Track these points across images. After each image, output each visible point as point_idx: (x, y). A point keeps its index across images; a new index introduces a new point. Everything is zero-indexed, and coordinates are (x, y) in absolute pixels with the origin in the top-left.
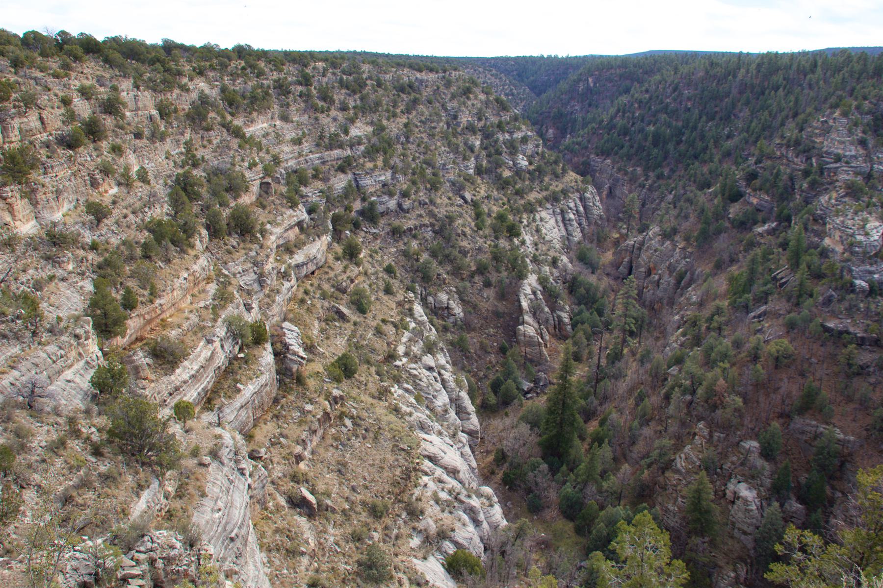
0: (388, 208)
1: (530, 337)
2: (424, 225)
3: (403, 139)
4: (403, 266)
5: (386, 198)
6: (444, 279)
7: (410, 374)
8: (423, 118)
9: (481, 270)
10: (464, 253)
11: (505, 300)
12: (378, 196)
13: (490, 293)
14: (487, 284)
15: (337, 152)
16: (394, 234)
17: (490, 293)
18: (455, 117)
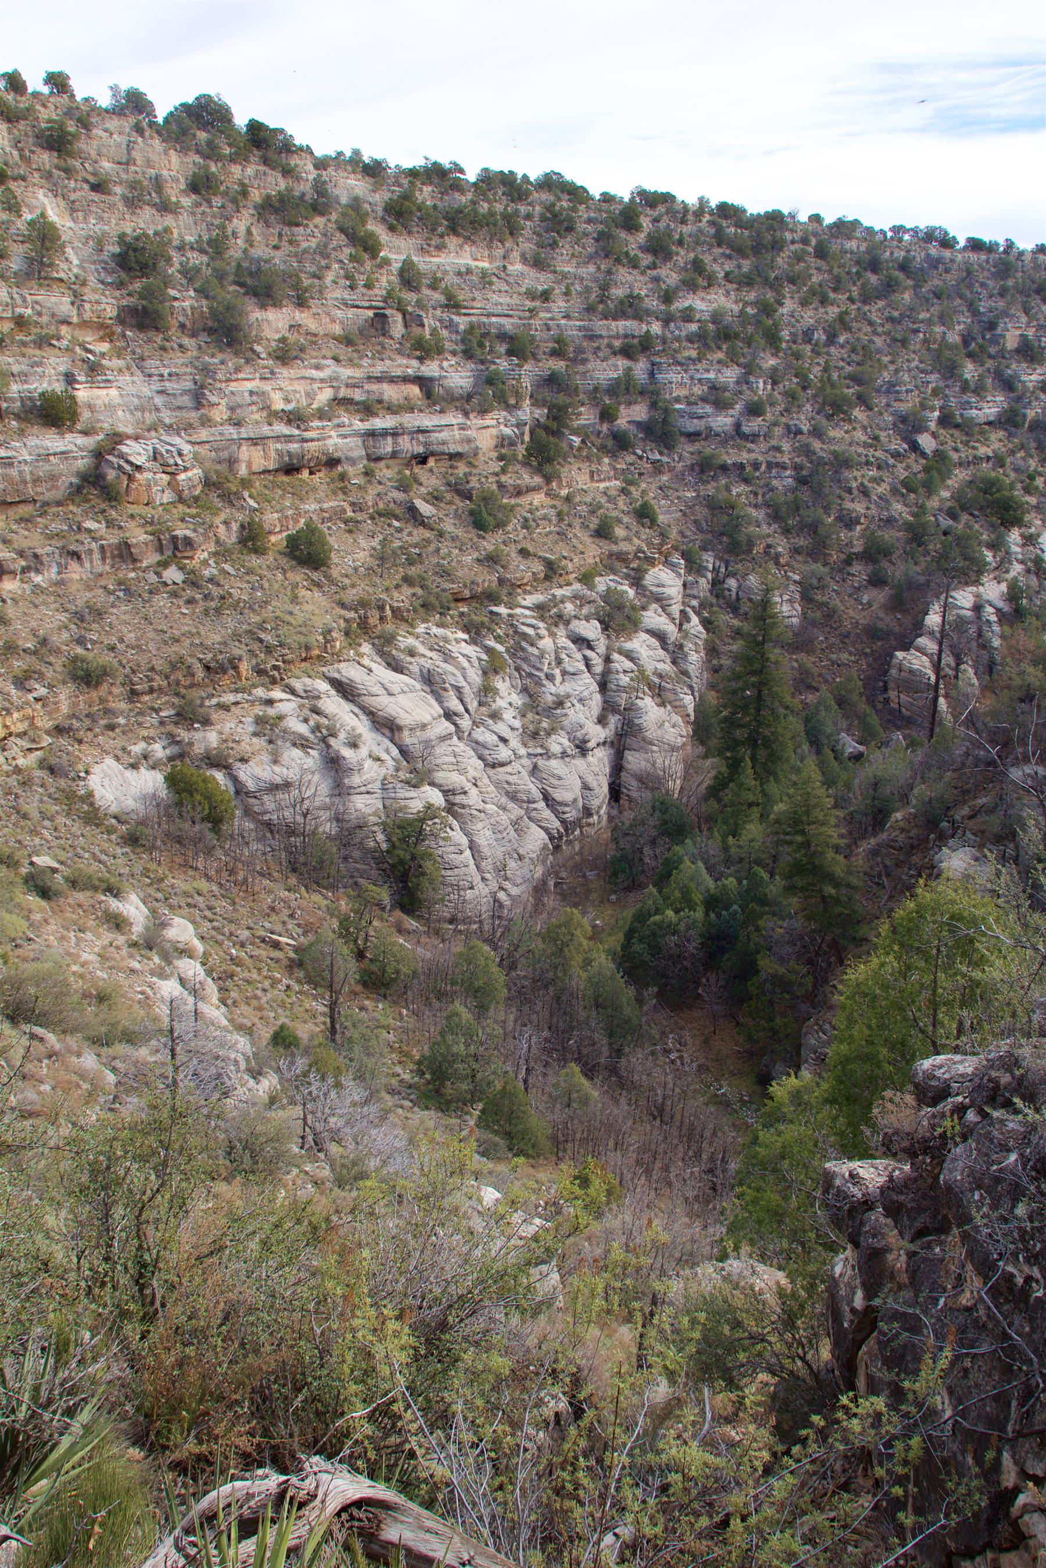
0: (710, 429)
1: (911, 671)
2: (777, 465)
3: (820, 336)
4: (695, 522)
5: (709, 409)
6: (778, 556)
7: (516, 632)
8: (896, 314)
9: (874, 553)
10: (848, 522)
11: (904, 611)
12: (689, 404)
13: (878, 596)
14: (877, 581)
15: (622, 326)
16: (702, 472)
17: (878, 596)
18: (992, 326)
